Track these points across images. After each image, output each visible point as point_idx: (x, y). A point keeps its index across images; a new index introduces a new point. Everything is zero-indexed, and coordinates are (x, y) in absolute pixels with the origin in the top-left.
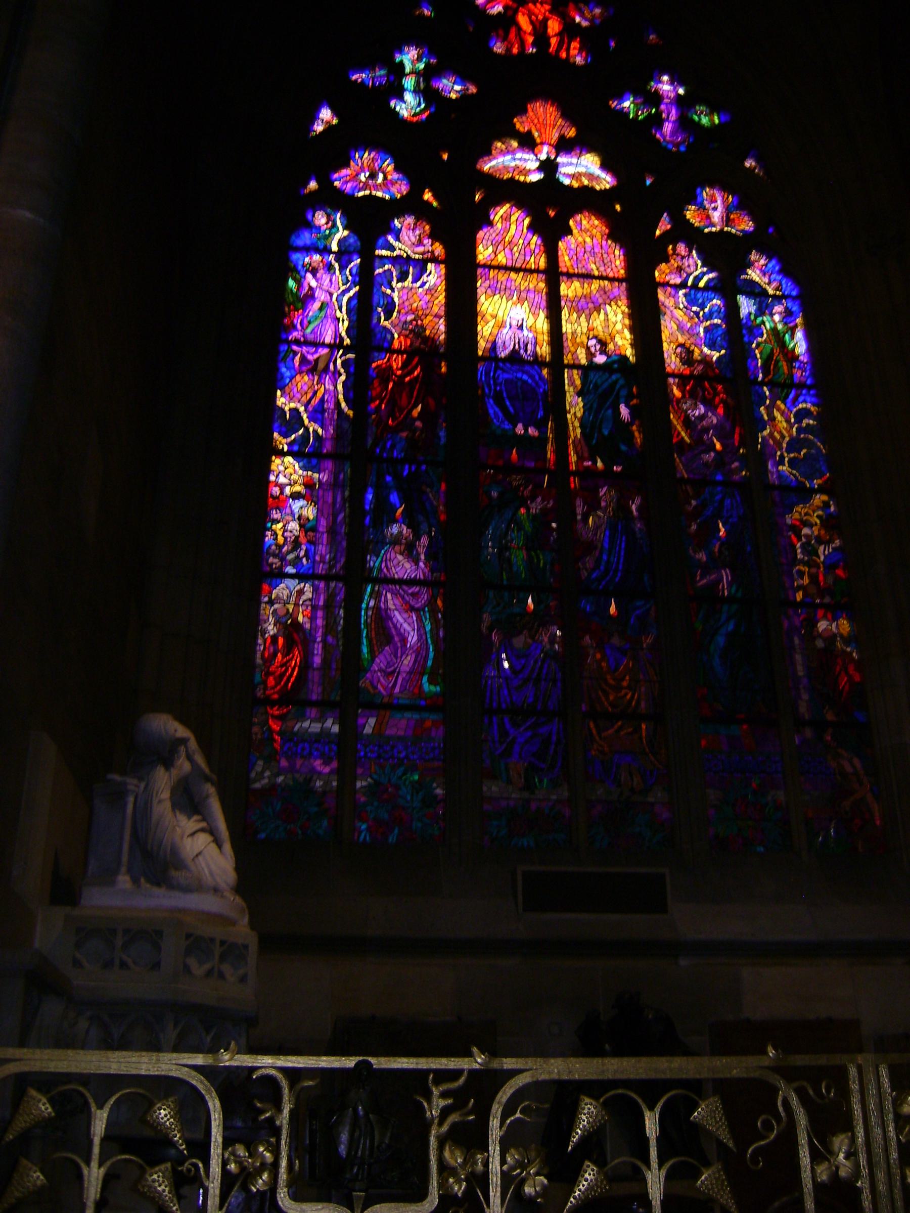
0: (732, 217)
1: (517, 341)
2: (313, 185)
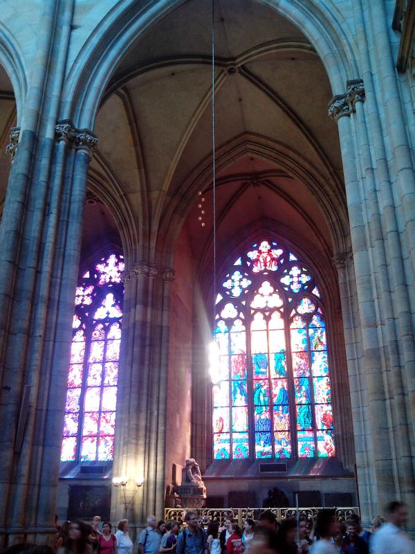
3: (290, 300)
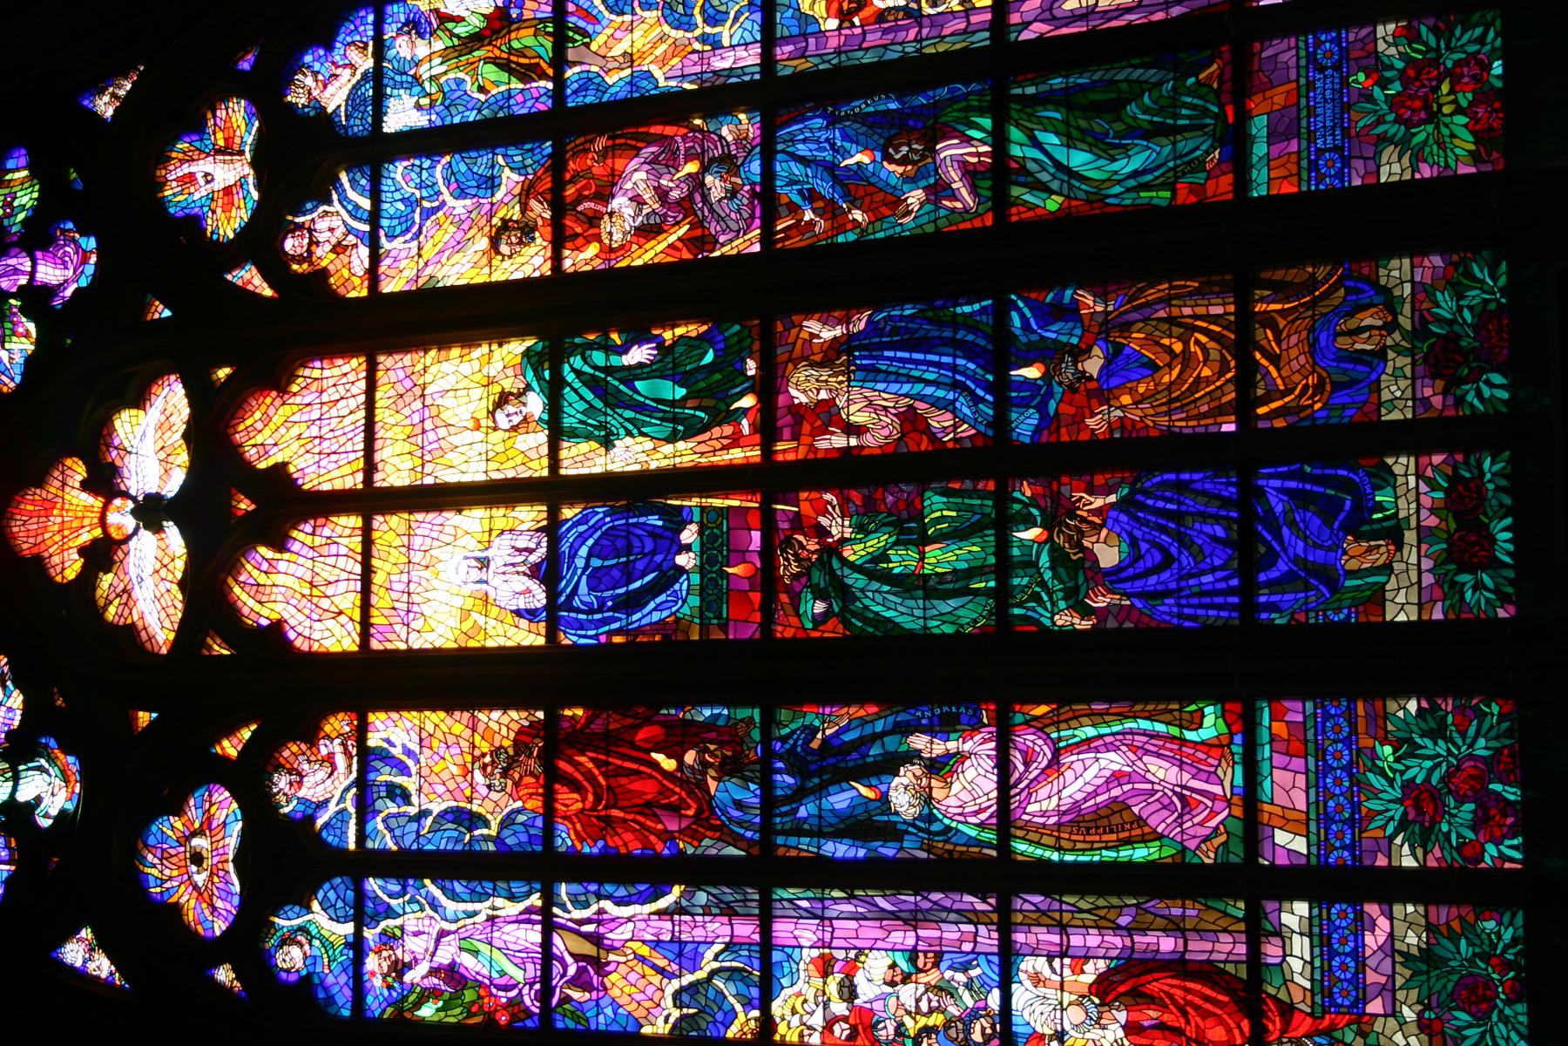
0: (221, 143)
1: (510, 569)
2: (224, 974)
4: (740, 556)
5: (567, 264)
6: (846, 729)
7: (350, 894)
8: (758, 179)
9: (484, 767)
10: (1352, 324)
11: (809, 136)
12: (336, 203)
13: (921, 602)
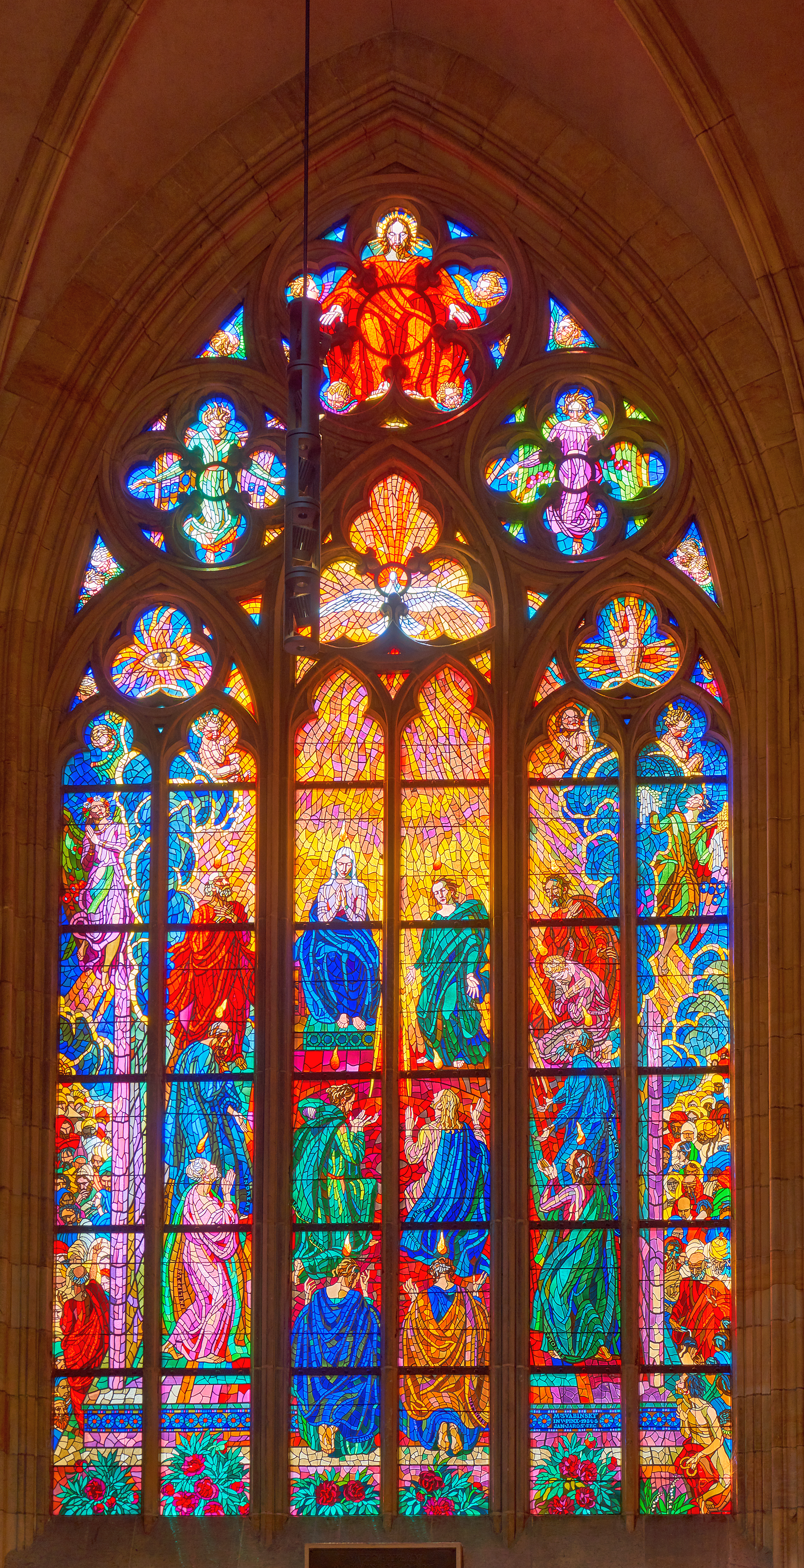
3: (535, 601)
4: (345, 1057)
5: (535, 930)
6: (239, 1130)
7: (140, 781)
8: (575, 1066)
9: (220, 880)
10: (454, 1433)
11: (599, 1100)
12: (595, 751)
13: (311, 1177)
